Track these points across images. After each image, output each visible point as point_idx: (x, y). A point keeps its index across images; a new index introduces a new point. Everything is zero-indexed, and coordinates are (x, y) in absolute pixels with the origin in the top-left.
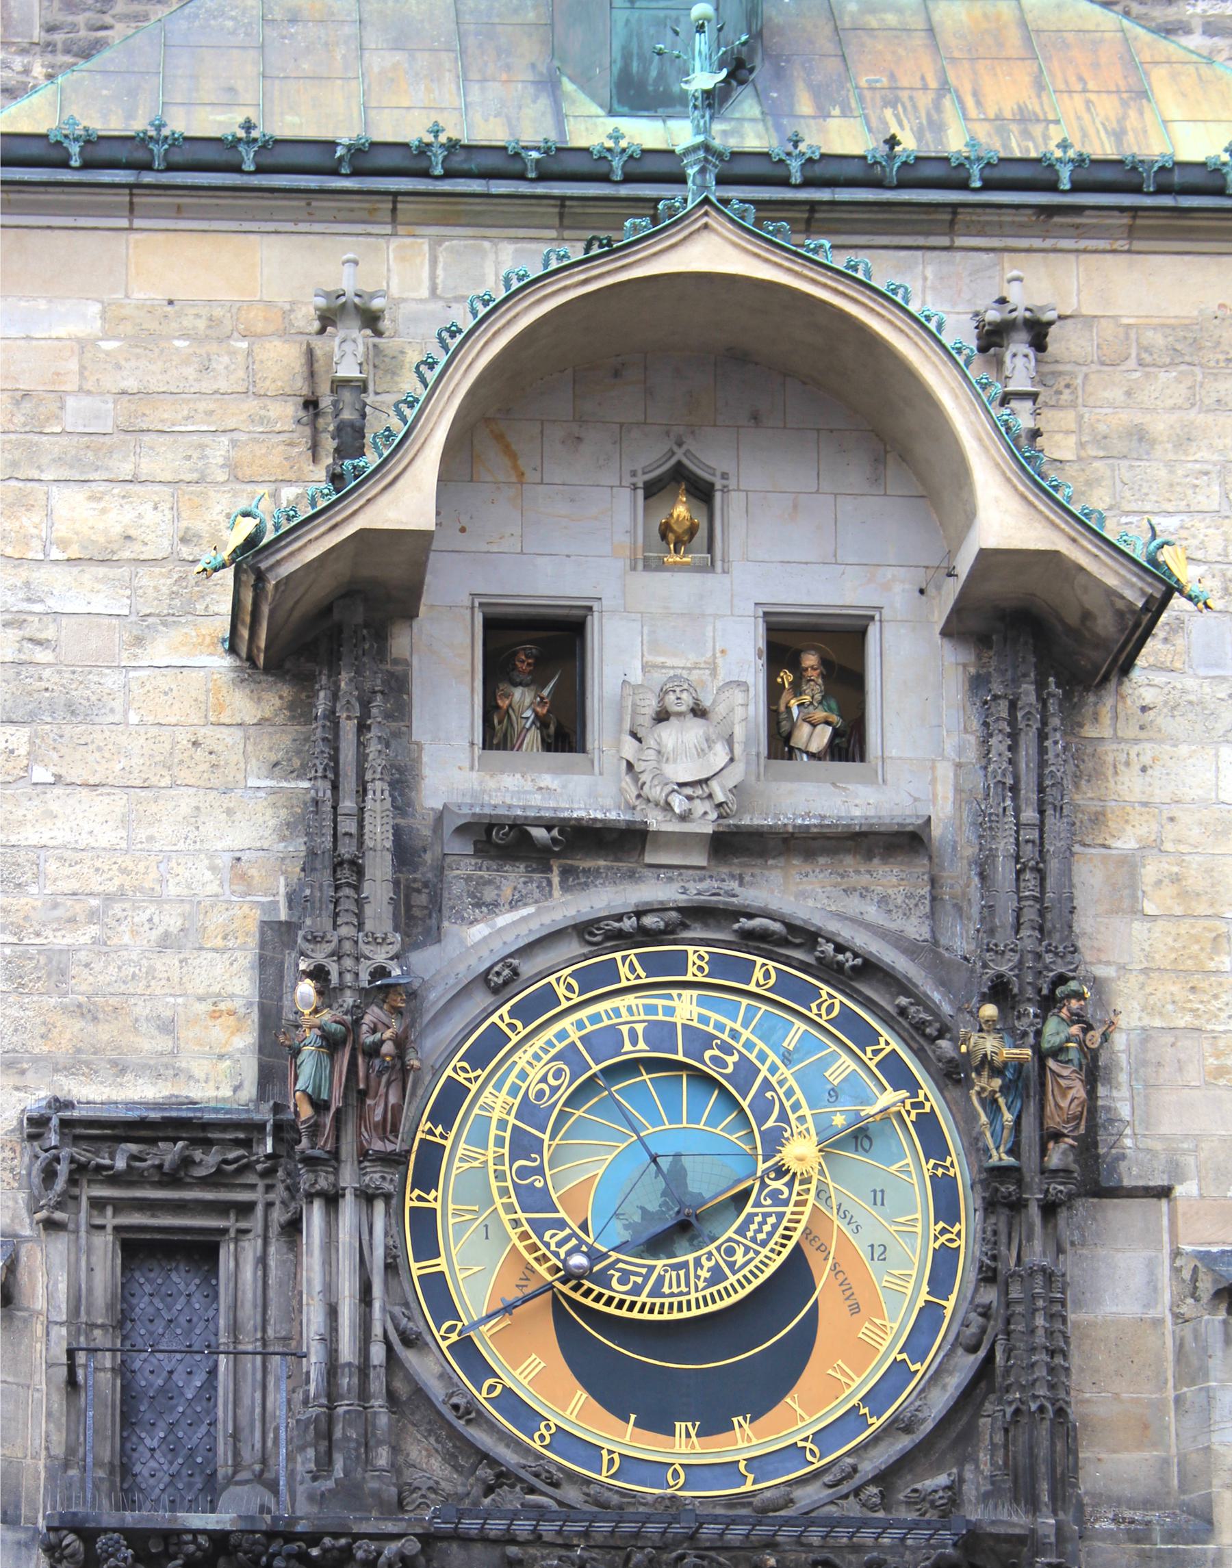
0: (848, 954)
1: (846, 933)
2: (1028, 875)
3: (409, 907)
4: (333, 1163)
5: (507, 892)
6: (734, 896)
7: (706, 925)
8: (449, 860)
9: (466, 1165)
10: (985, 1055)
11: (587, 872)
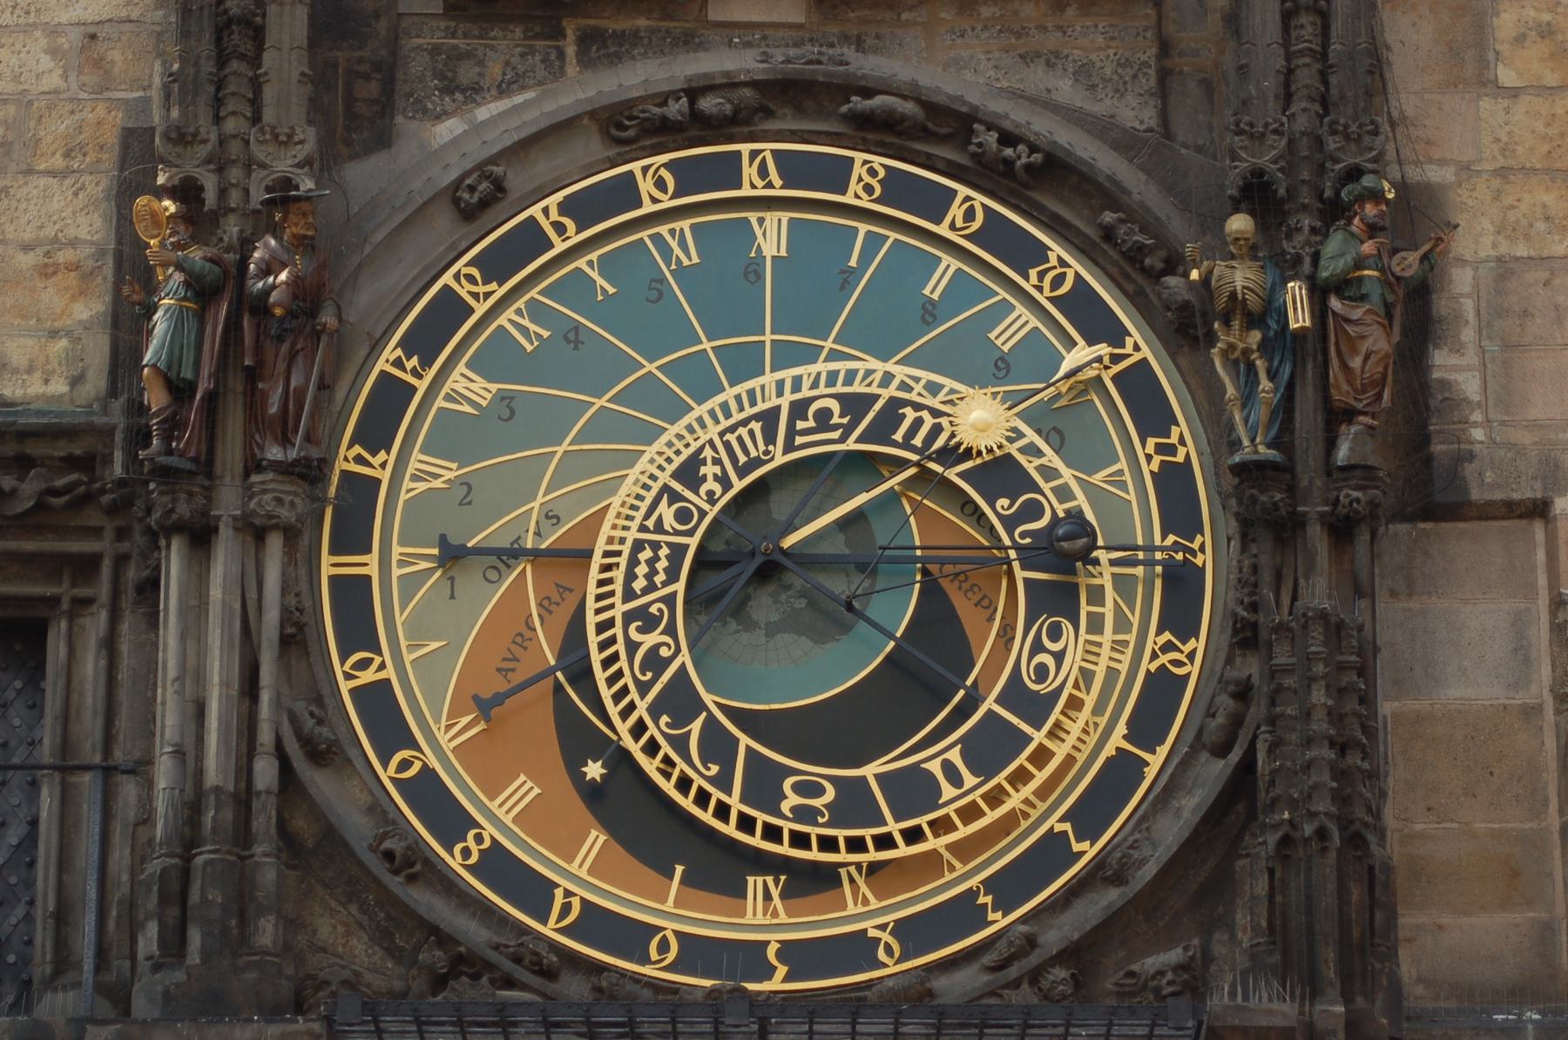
0: (1021, 148)
1: (1018, 116)
2: (1304, 19)
3: (350, 101)
4: (201, 479)
5: (495, 70)
6: (841, 63)
7: (801, 111)
8: (405, 23)
9: (422, 486)
10: (1233, 294)
11: (620, 37)
